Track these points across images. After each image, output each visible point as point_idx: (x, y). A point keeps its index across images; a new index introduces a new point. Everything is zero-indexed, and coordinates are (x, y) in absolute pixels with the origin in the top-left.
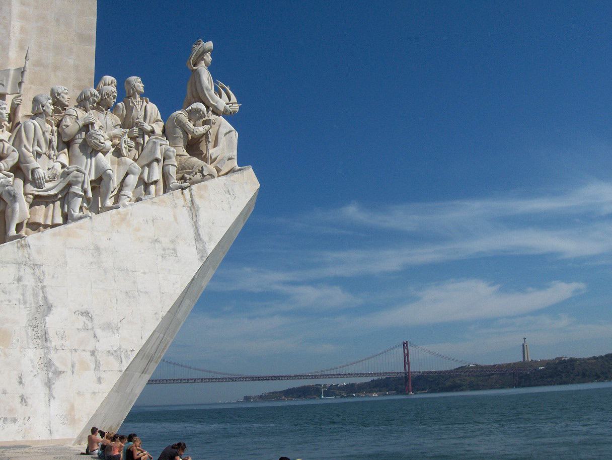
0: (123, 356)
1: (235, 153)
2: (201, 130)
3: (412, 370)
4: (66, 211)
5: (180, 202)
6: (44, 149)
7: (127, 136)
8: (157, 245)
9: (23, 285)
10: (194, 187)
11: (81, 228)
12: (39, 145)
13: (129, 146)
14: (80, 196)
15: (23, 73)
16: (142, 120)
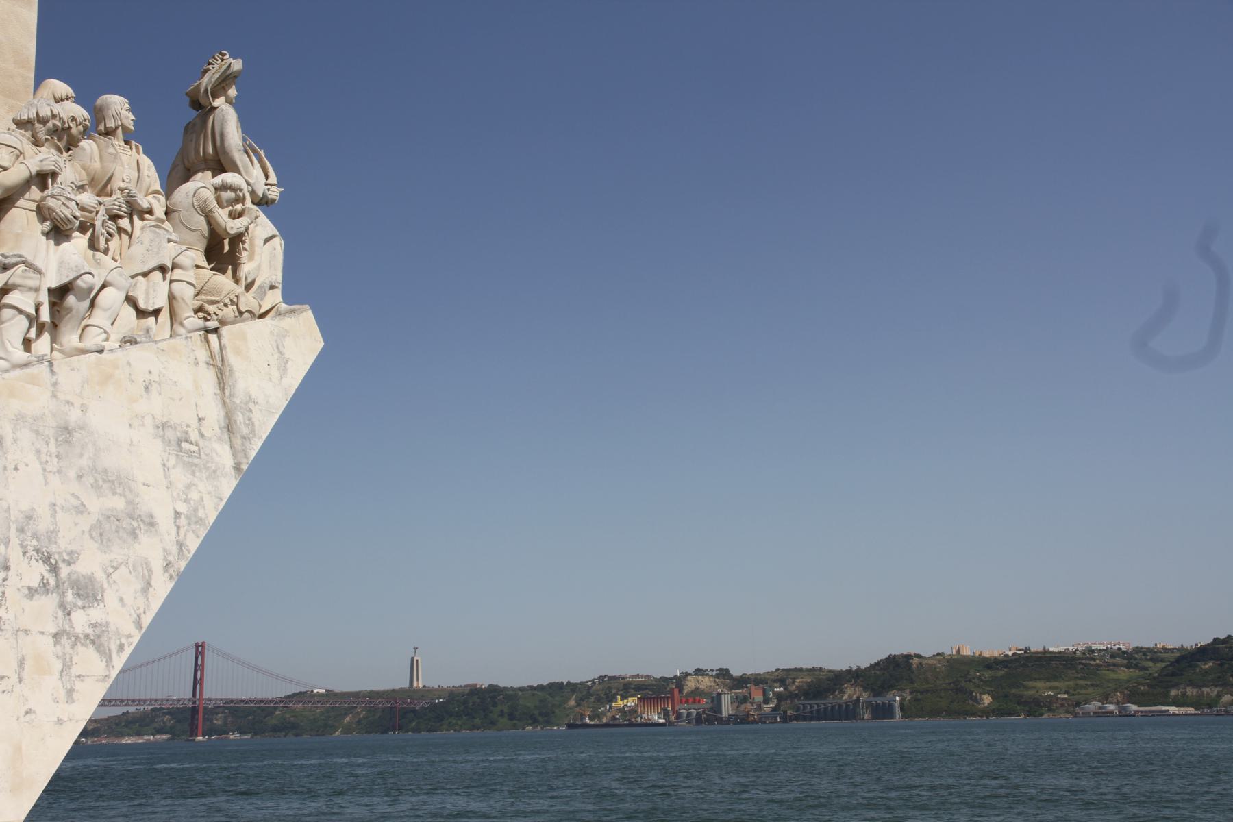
0: (114, 647)
1: (278, 277)
2: (234, 226)
3: (207, 695)
5: (202, 355)
8: (169, 434)
11: (34, 381)
14: (28, 316)
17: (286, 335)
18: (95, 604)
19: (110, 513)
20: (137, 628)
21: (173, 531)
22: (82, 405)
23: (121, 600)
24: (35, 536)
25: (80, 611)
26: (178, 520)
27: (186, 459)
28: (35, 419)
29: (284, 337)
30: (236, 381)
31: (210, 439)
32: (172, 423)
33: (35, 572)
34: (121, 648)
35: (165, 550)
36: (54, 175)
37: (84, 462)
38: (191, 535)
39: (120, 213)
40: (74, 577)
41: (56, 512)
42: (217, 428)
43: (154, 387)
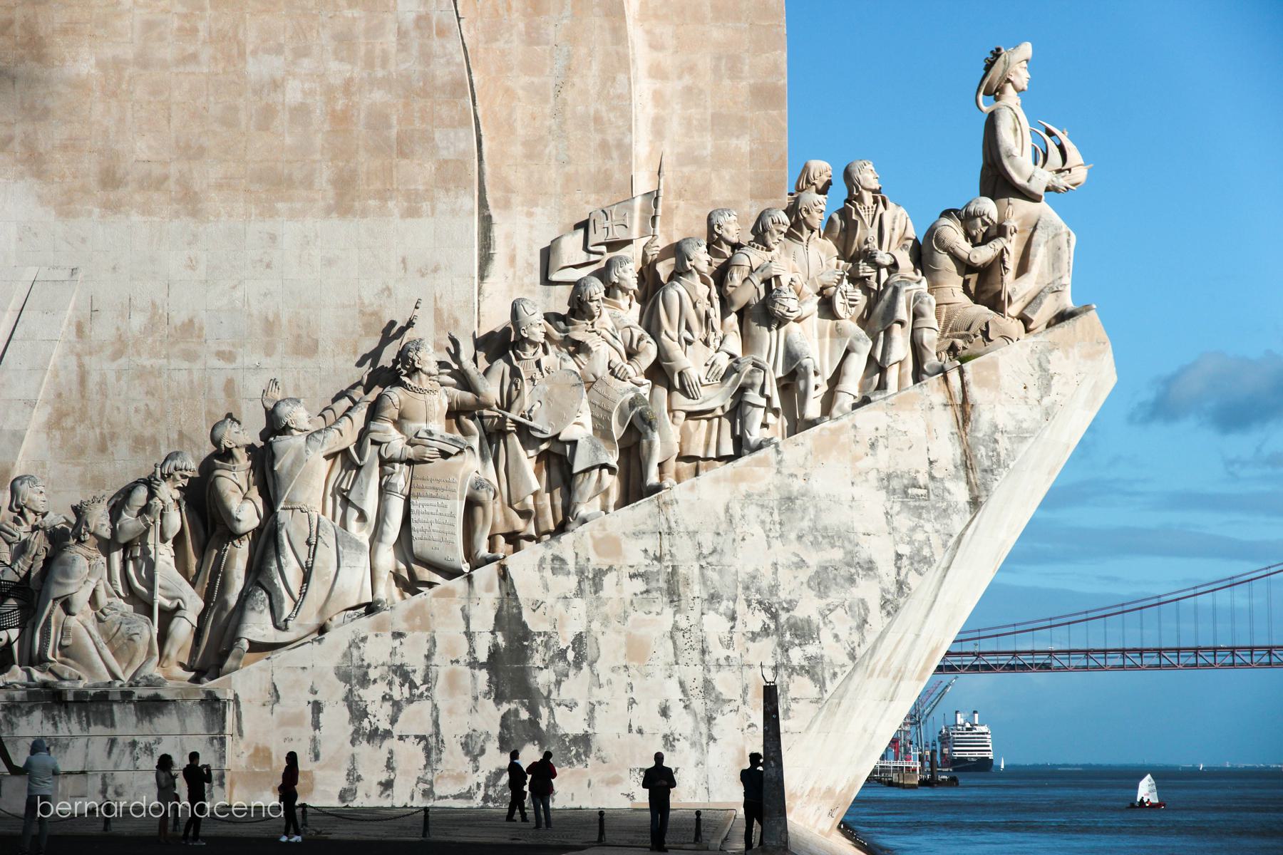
0: (827, 675)
2: (983, 255)
4: (738, 433)
5: (939, 397)
6: (699, 333)
7: (845, 281)
8: (896, 484)
9: (668, 567)
10: (968, 366)
11: (760, 463)
12: (688, 328)
13: (850, 300)
15: (656, 199)
16: (874, 244)
17: (1053, 349)
18: (811, 642)
19: (828, 564)
20: (850, 659)
21: (893, 571)
22: (805, 475)
23: (836, 636)
24: (758, 591)
25: (797, 648)
26: (899, 562)
27: (912, 503)
28: (760, 496)
29: (1050, 351)
30: (979, 415)
31: (942, 480)
32: (899, 472)
33: (757, 620)
34: (835, 675)
35: (883, 590)
36: (777, 277)
37: (806, 524)
38: (912, 574)
39: (865, 274)
40: (792, 621)
41: (777, 569)
42: (951, 468)
43: (881, 442)
